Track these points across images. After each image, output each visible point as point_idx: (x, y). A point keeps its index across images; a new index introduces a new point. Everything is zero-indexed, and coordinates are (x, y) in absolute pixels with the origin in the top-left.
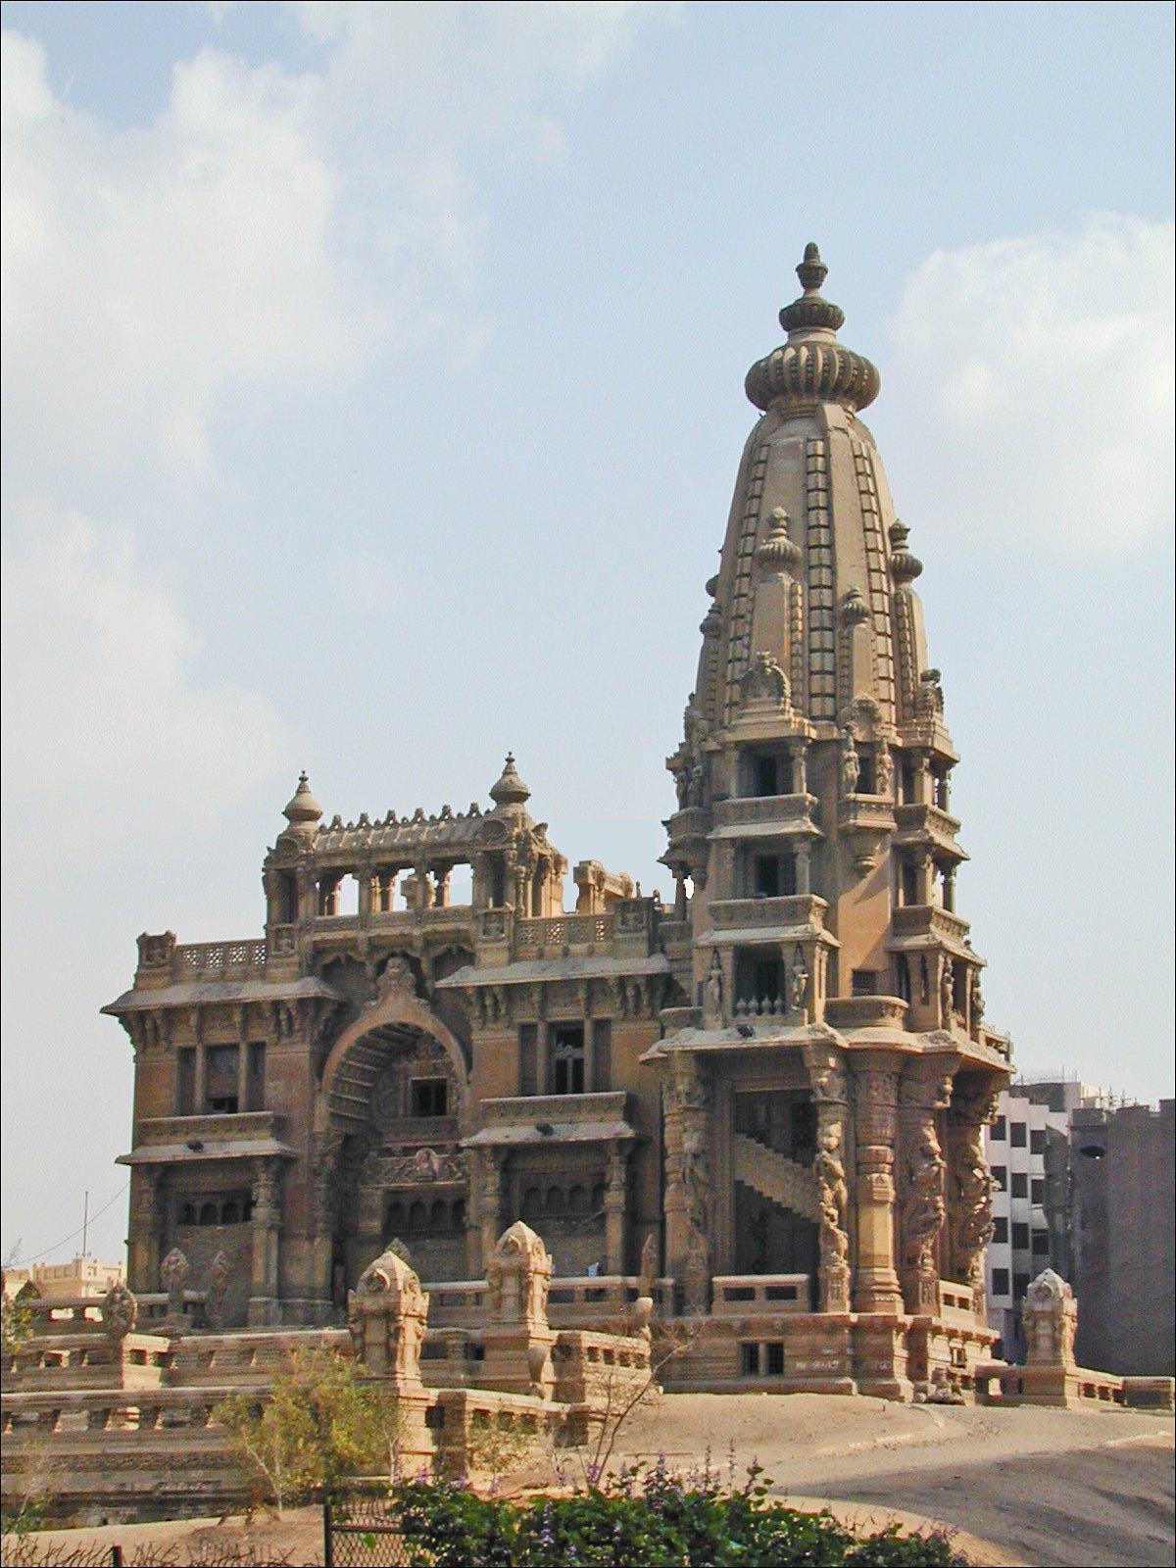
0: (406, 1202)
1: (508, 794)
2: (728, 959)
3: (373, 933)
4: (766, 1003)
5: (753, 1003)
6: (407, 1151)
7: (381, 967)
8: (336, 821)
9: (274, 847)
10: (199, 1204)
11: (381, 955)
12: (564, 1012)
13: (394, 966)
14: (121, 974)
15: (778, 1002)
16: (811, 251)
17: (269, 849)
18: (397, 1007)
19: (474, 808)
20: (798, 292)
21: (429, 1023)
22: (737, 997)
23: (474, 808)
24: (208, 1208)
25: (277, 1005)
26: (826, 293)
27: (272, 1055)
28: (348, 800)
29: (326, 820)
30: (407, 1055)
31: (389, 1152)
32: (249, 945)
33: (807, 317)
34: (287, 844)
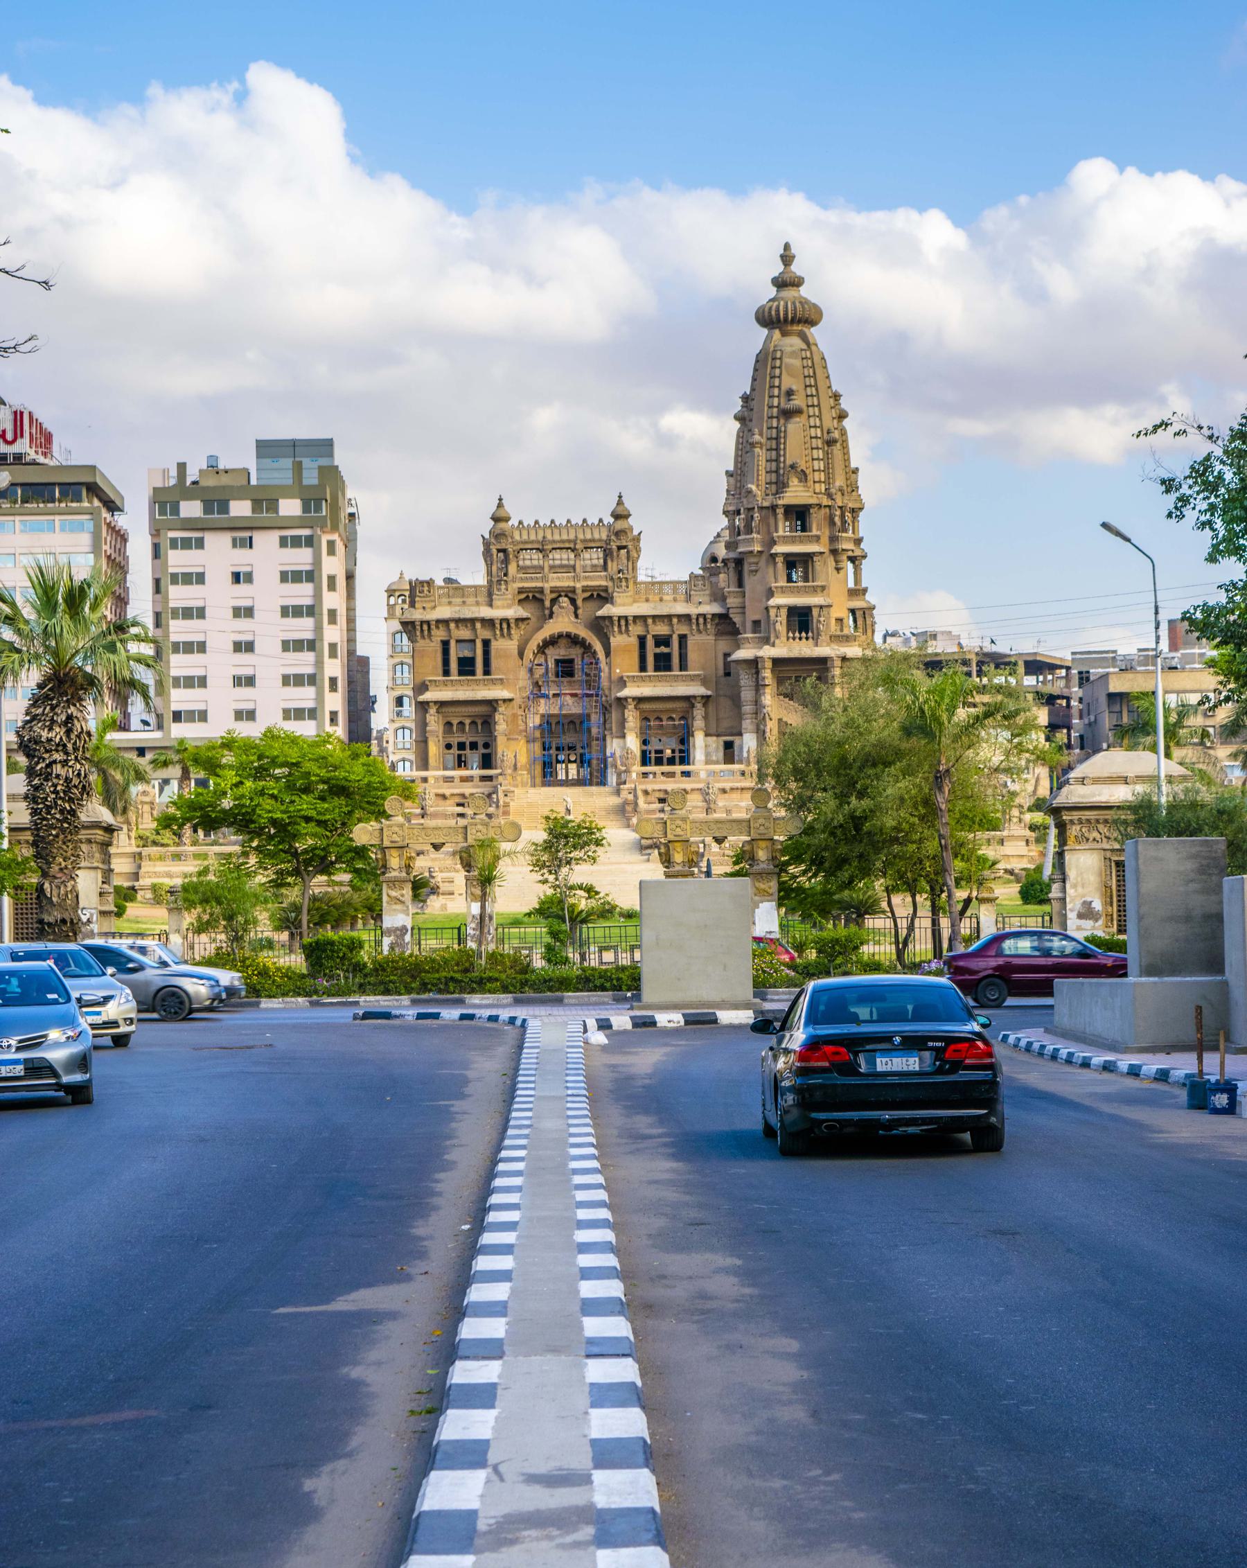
0: (553, 722)
2: (784, 612)
4: (804, 634)
5: (797, 635)
7: (554, 601)
9: (487, 536)
10: (455, 722)
11: (554, 595)
12: (661, 629)
15: (810, 634)
16: (787, 247)
18: (563, 623)
19: (601, 520)
20: (780, 268)
21: (584, 633)
24: (461, 723)
26: (796, 268)
27: (495, 645)
28: (521, 513)
29: (514, 522)
34: (498, 535)
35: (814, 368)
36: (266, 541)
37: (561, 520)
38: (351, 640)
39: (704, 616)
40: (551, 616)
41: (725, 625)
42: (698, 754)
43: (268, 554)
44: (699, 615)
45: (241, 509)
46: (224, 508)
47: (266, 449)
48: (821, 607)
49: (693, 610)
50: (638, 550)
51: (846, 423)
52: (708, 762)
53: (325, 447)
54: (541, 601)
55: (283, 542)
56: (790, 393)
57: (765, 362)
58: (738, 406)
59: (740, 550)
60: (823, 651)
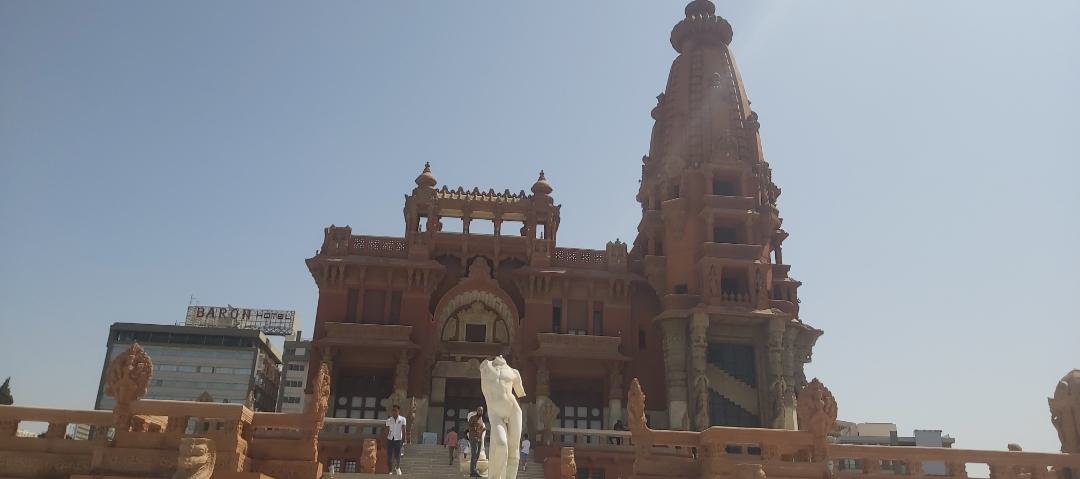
1: (541, 190)
7: (470, 262)
8: (445, 188)
9: (410, 194)
13: (480, 262)
14: (314, 245)
17: (406, 196)
19: (522, 193)
22: (723, 293)
23: (522, 193)
28: (449, 178)
30: (466, 309)
31: (453, 359)
32: (396, 240)
40: (466, 276)
50: (557, 220)
54: (460, 260)
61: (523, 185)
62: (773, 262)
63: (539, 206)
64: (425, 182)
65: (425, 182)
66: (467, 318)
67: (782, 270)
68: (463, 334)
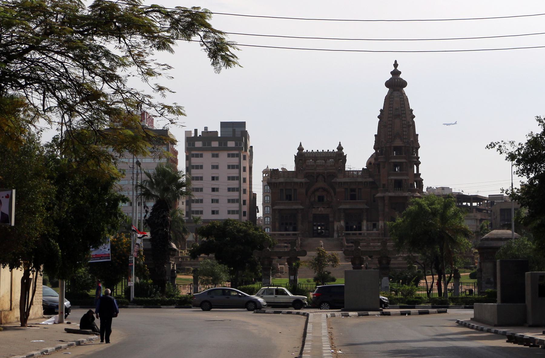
1: (340, 148)
2: (393, 181)
3: (318, 171)
6: (318, 208)
16: (396, 61)
18: (321, 184)
25: (301, 183)
26: (399, 68)
28: (307, 148)
31: (314, 208)
33: (396, 73)
35: (404, 101)
36: (223, 155)
37: (320, 150)
38: (251, 188)
39: (367, 182)
41: (374, 185)
42: (364, 228)
43: (224, 159)
44: (365, 182)
45: (215, 144)
46: (210, 144)
47: (223, 125)
48: (405, 180)
49: (364, 180)
51: (414, 119)
52: (367, 230)
53: (243, 124)
55: (229, 156)
56: (396, 109)
57: (388, 99)
58: (379, 113)
59: (379, 160)
60: (407, 194)
61: (333, 148)
62: (415, 172)
63: (339, 157)
64: (300, 149)
65: (300, 149)
66: (318, 194)
67: (418, 175)
68: (317, 199)
